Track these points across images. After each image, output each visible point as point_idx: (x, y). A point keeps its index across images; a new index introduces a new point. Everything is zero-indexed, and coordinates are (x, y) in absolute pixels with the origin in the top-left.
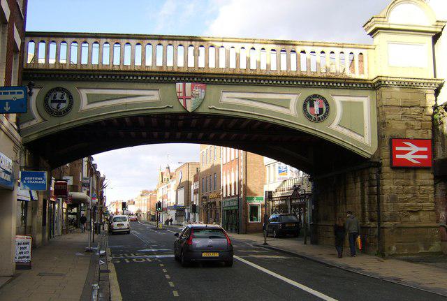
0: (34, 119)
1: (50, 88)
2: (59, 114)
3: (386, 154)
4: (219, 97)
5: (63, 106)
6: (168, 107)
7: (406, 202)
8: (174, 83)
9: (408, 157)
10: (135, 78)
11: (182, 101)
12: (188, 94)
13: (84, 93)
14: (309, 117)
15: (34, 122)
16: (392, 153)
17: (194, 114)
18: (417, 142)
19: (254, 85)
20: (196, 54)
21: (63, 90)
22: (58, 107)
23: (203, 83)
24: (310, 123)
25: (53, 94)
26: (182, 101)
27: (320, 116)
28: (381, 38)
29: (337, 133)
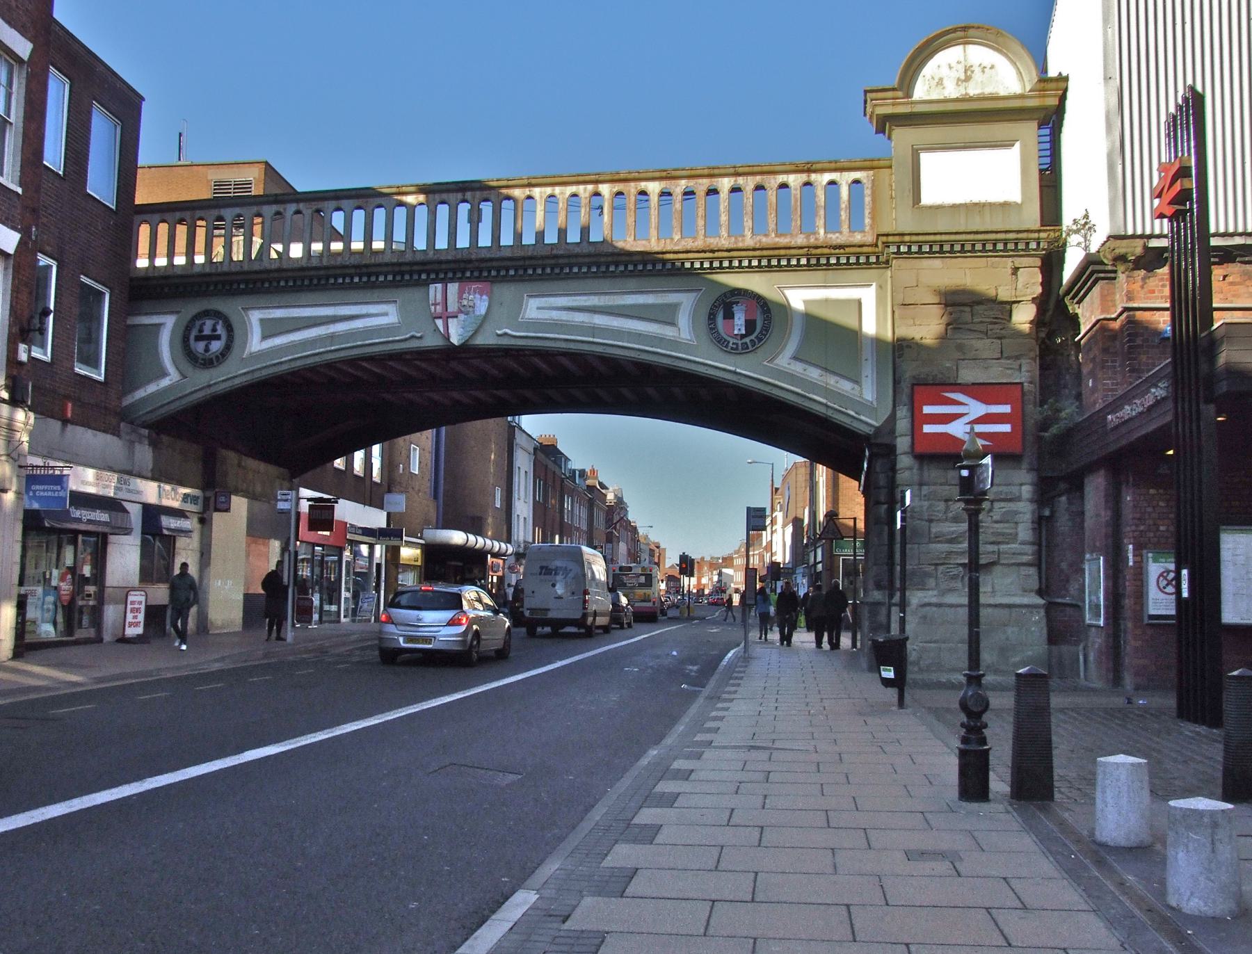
0: (164, 374)
1: (189, 317)
2: (208, 363)
3: (903, 425)
4: (519, 306)
5: (216, 346)
6: (413, 337)
7: (951, 541)
8: (426, 284)
9: (957, 429)
10: (348, 280)
11: (439, 323)
12: (453, 306)
13: (255, 316)
14: (720, 342)
15: (165, 382)
16: (917, 419)
17: (466, 351)
18: (981, 391)
19: (596, 276)
20: (475, 219)
21: (217, 315)
22: (207, 349)
23: (486, 280)
24: (722, 355)
25: (198, 323)
26: (439, 323)
27: (747, 340)
28: (903, 137)
29: (792, 378)
